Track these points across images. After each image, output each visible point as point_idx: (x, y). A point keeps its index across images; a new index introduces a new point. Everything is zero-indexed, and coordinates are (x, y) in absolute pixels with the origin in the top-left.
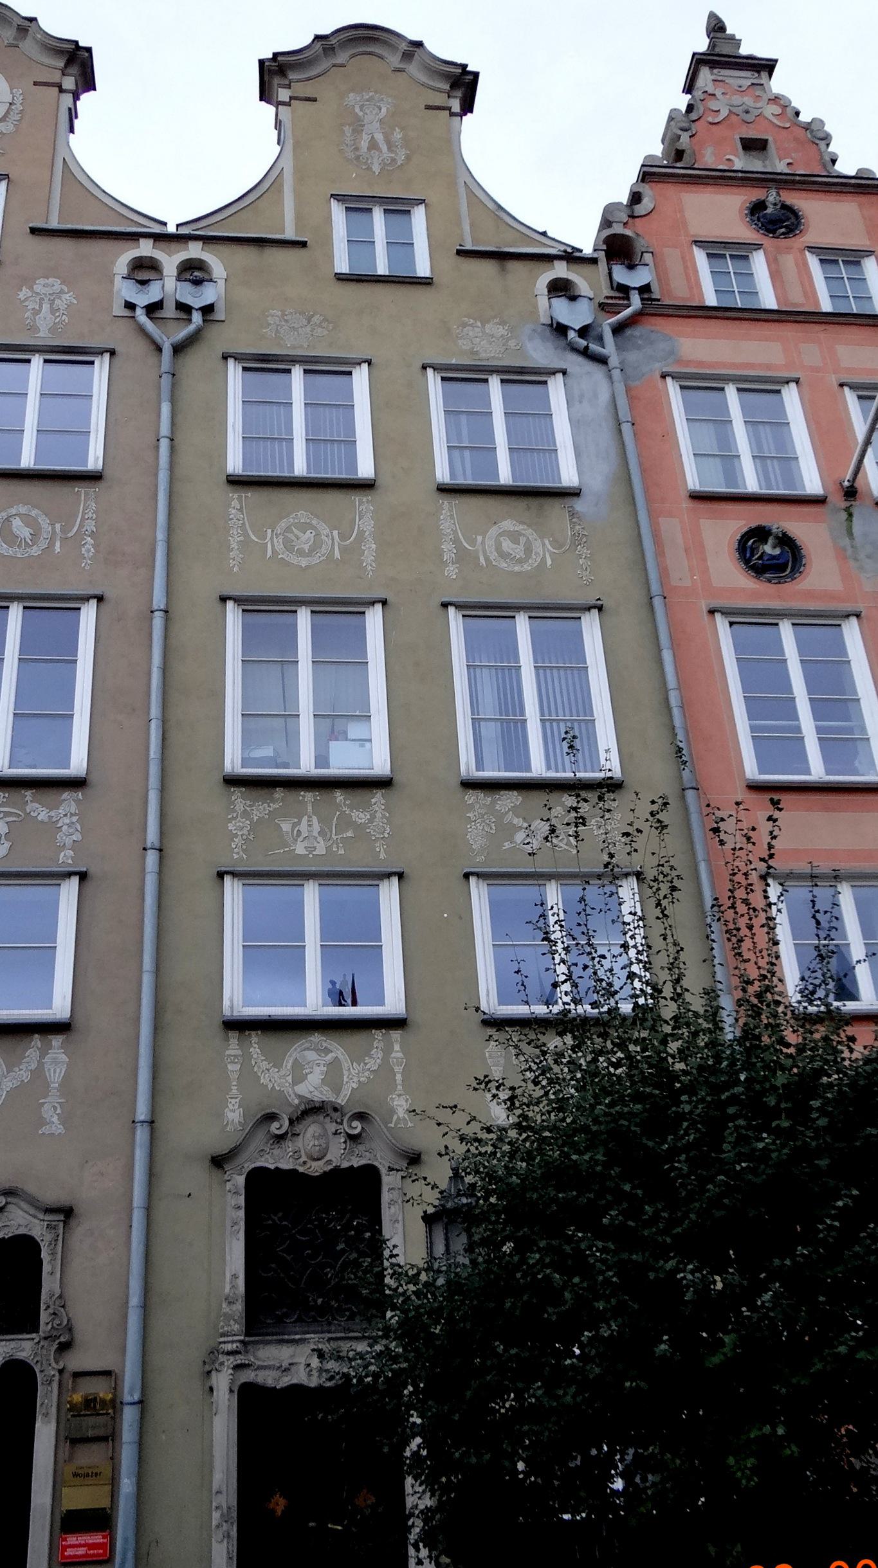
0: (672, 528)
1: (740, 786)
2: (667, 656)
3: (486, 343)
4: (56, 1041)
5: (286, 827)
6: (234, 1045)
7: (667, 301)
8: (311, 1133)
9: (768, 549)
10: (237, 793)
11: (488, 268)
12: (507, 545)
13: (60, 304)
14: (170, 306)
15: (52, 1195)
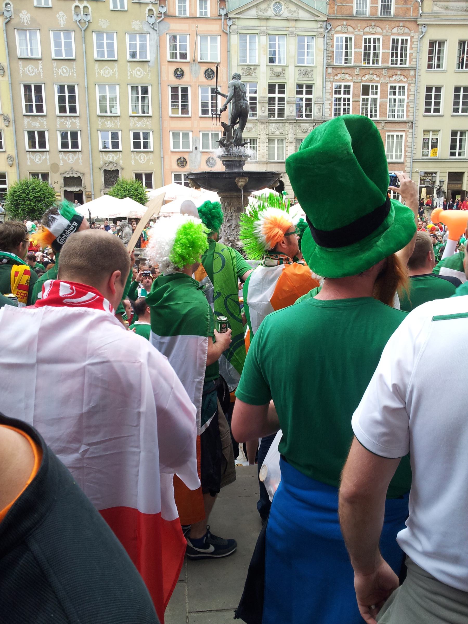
0: (164, 68)
1: (168, 117)
2: (160, 94)
3: (136, 26)
4: (80, 153)
5: (106, 123)
6: (101, 154)
7: (169, 14)
8: (110, 165)
9: (179, 73)
10: (99, 118)
11: (137, 6)
12: (138, 72)
13: (64, 18)
14: (82, 21)
15: (82, 172)
